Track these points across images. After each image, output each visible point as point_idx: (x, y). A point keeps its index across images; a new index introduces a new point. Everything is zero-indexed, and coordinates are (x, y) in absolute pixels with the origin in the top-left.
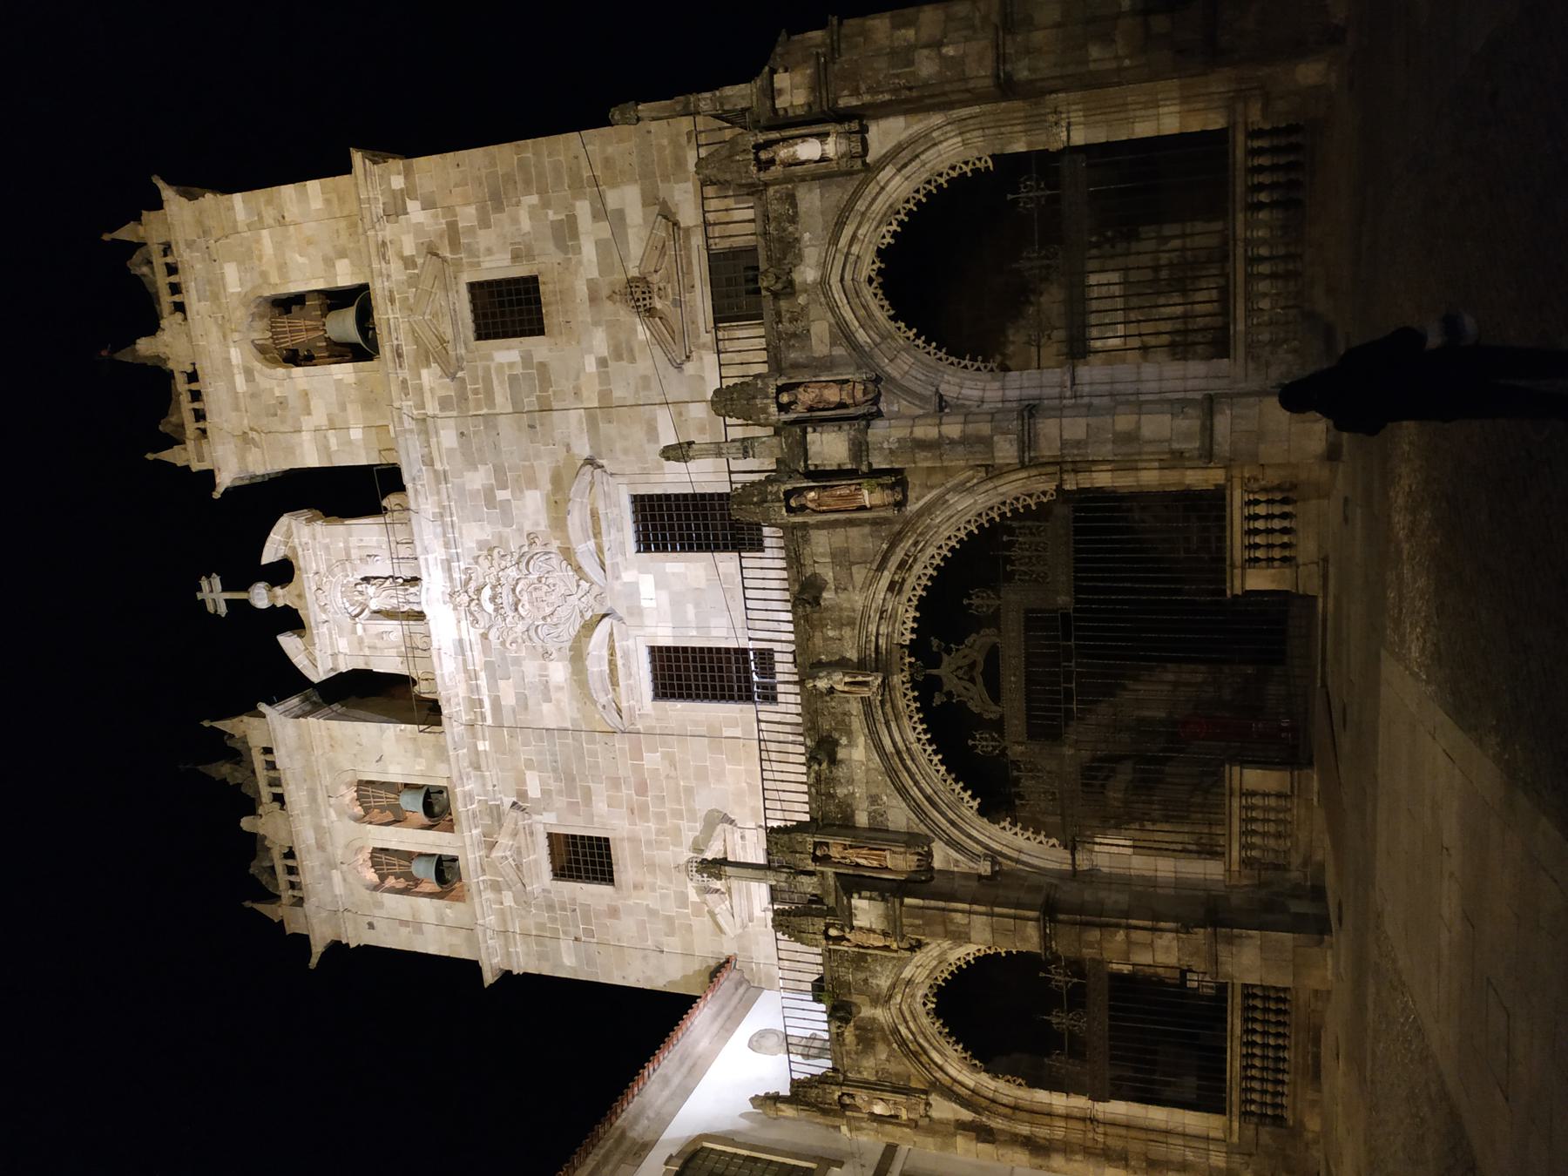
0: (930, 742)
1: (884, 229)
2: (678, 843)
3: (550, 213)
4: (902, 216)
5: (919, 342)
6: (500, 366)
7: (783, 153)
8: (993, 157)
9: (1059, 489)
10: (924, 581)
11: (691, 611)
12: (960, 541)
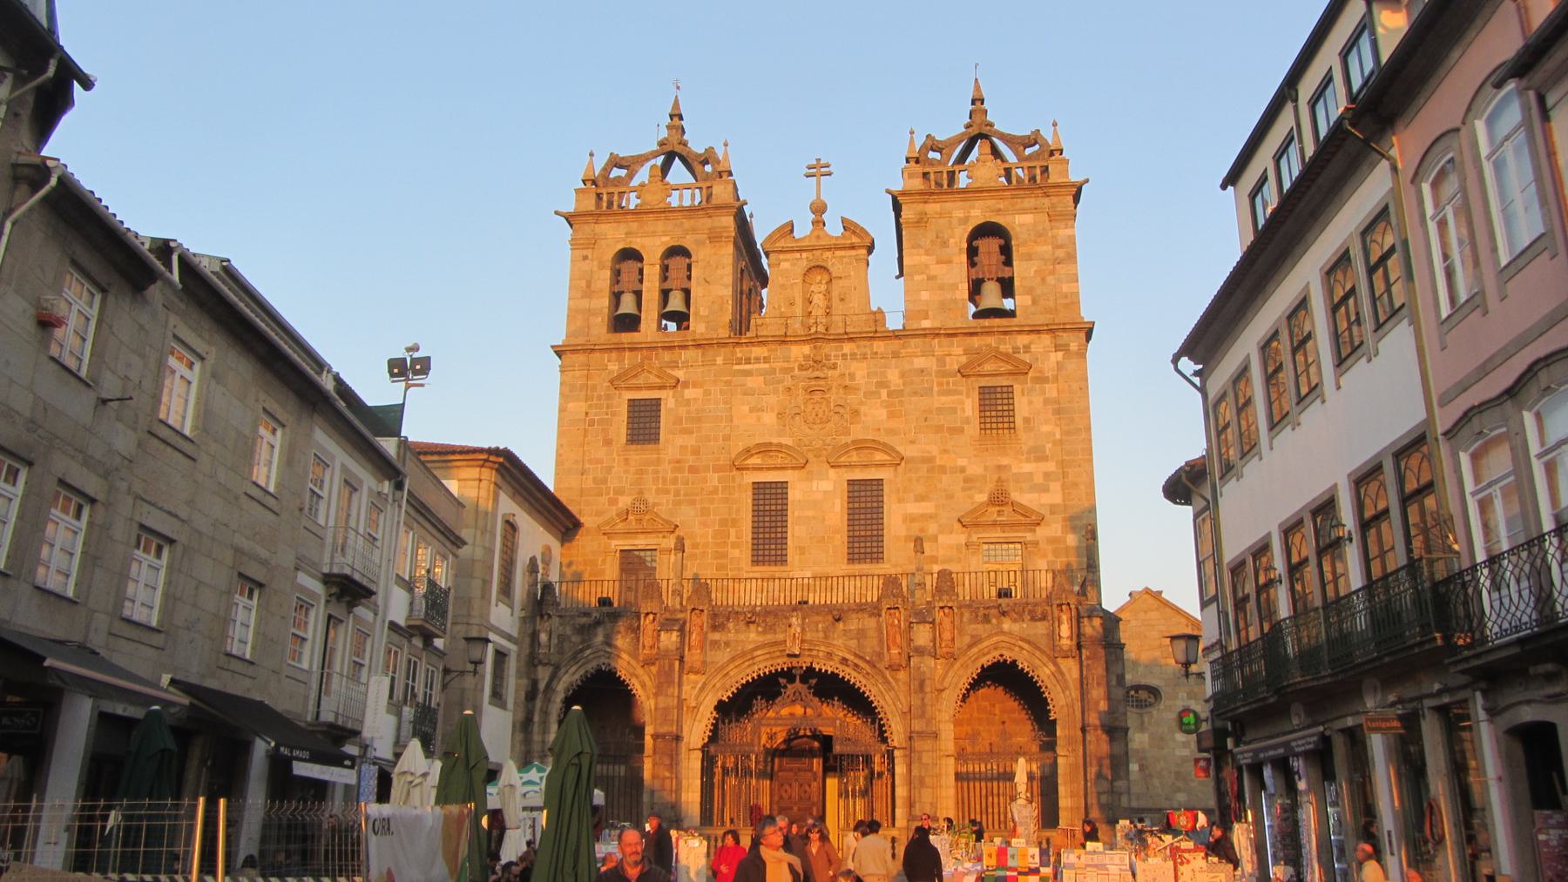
0: (759, 676)
1: (1026, 664)
2: (658, 491)
3: (1050, 445)
4: (1031, 674)
5: (970, 680)
6: (963, 403)
7: (1064, 617)
8: (1055, 720)
9: (895, 748)
10: (847, 677)
11: (810, 513)
12: (868, 697)
